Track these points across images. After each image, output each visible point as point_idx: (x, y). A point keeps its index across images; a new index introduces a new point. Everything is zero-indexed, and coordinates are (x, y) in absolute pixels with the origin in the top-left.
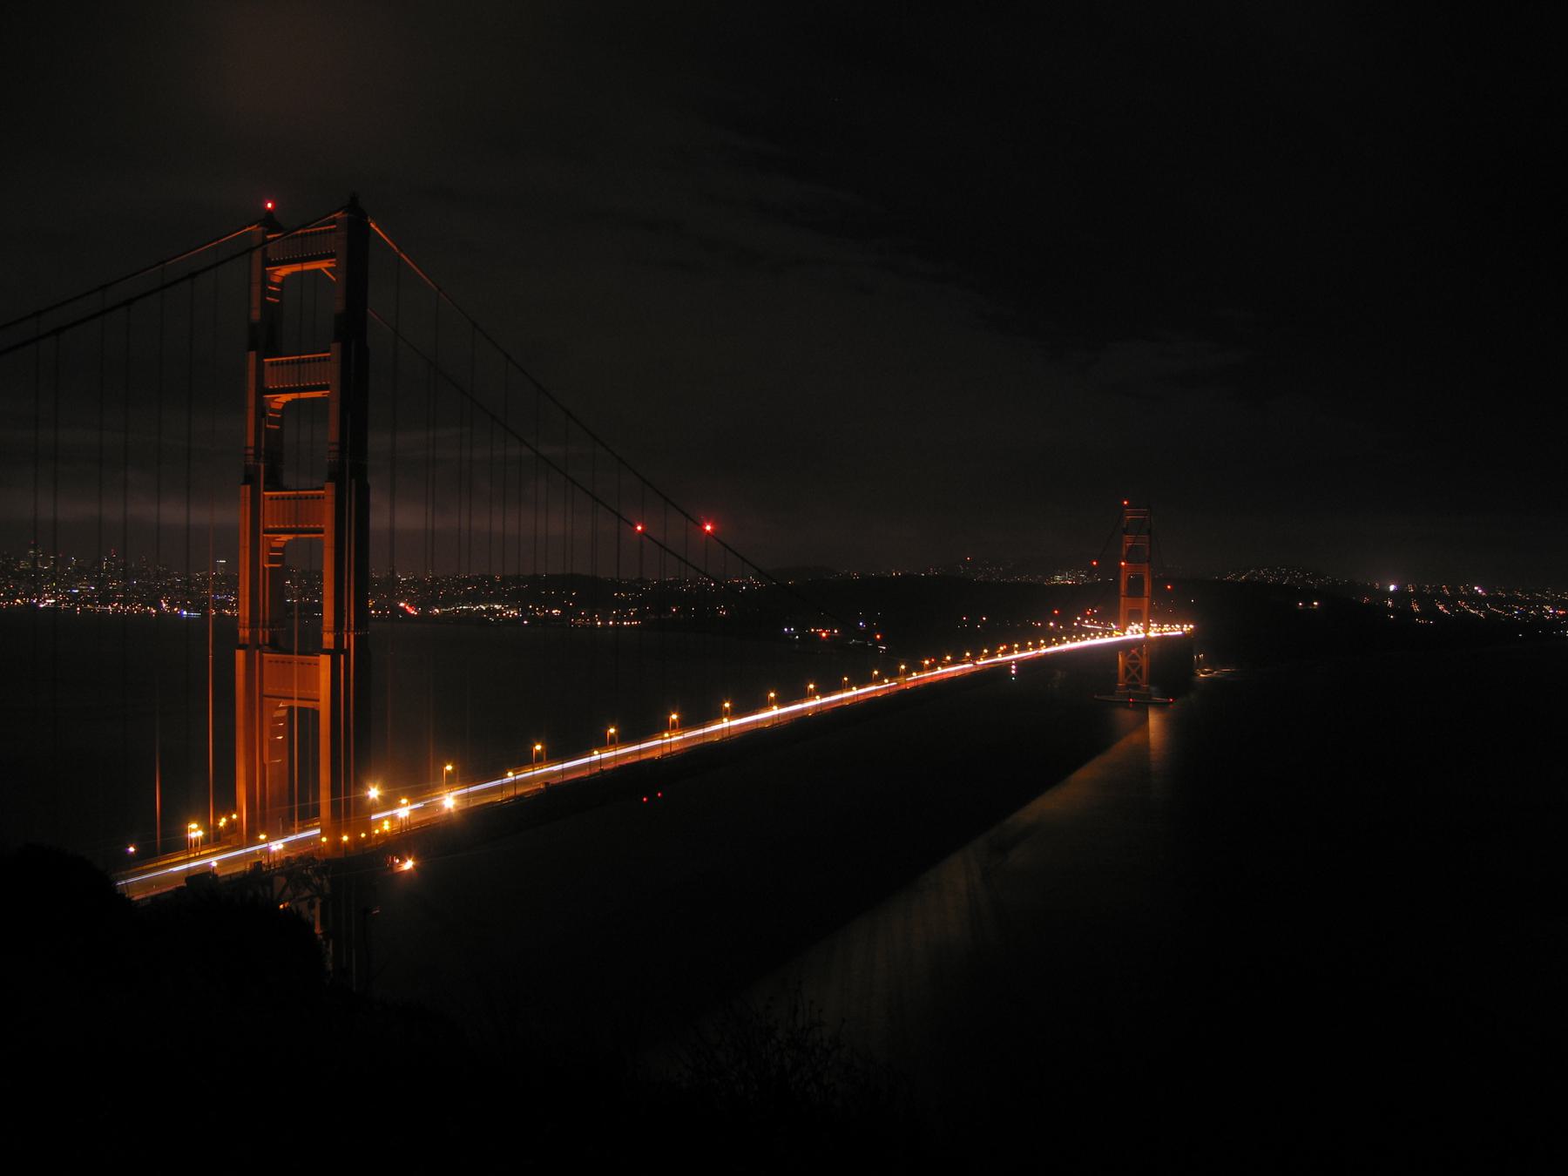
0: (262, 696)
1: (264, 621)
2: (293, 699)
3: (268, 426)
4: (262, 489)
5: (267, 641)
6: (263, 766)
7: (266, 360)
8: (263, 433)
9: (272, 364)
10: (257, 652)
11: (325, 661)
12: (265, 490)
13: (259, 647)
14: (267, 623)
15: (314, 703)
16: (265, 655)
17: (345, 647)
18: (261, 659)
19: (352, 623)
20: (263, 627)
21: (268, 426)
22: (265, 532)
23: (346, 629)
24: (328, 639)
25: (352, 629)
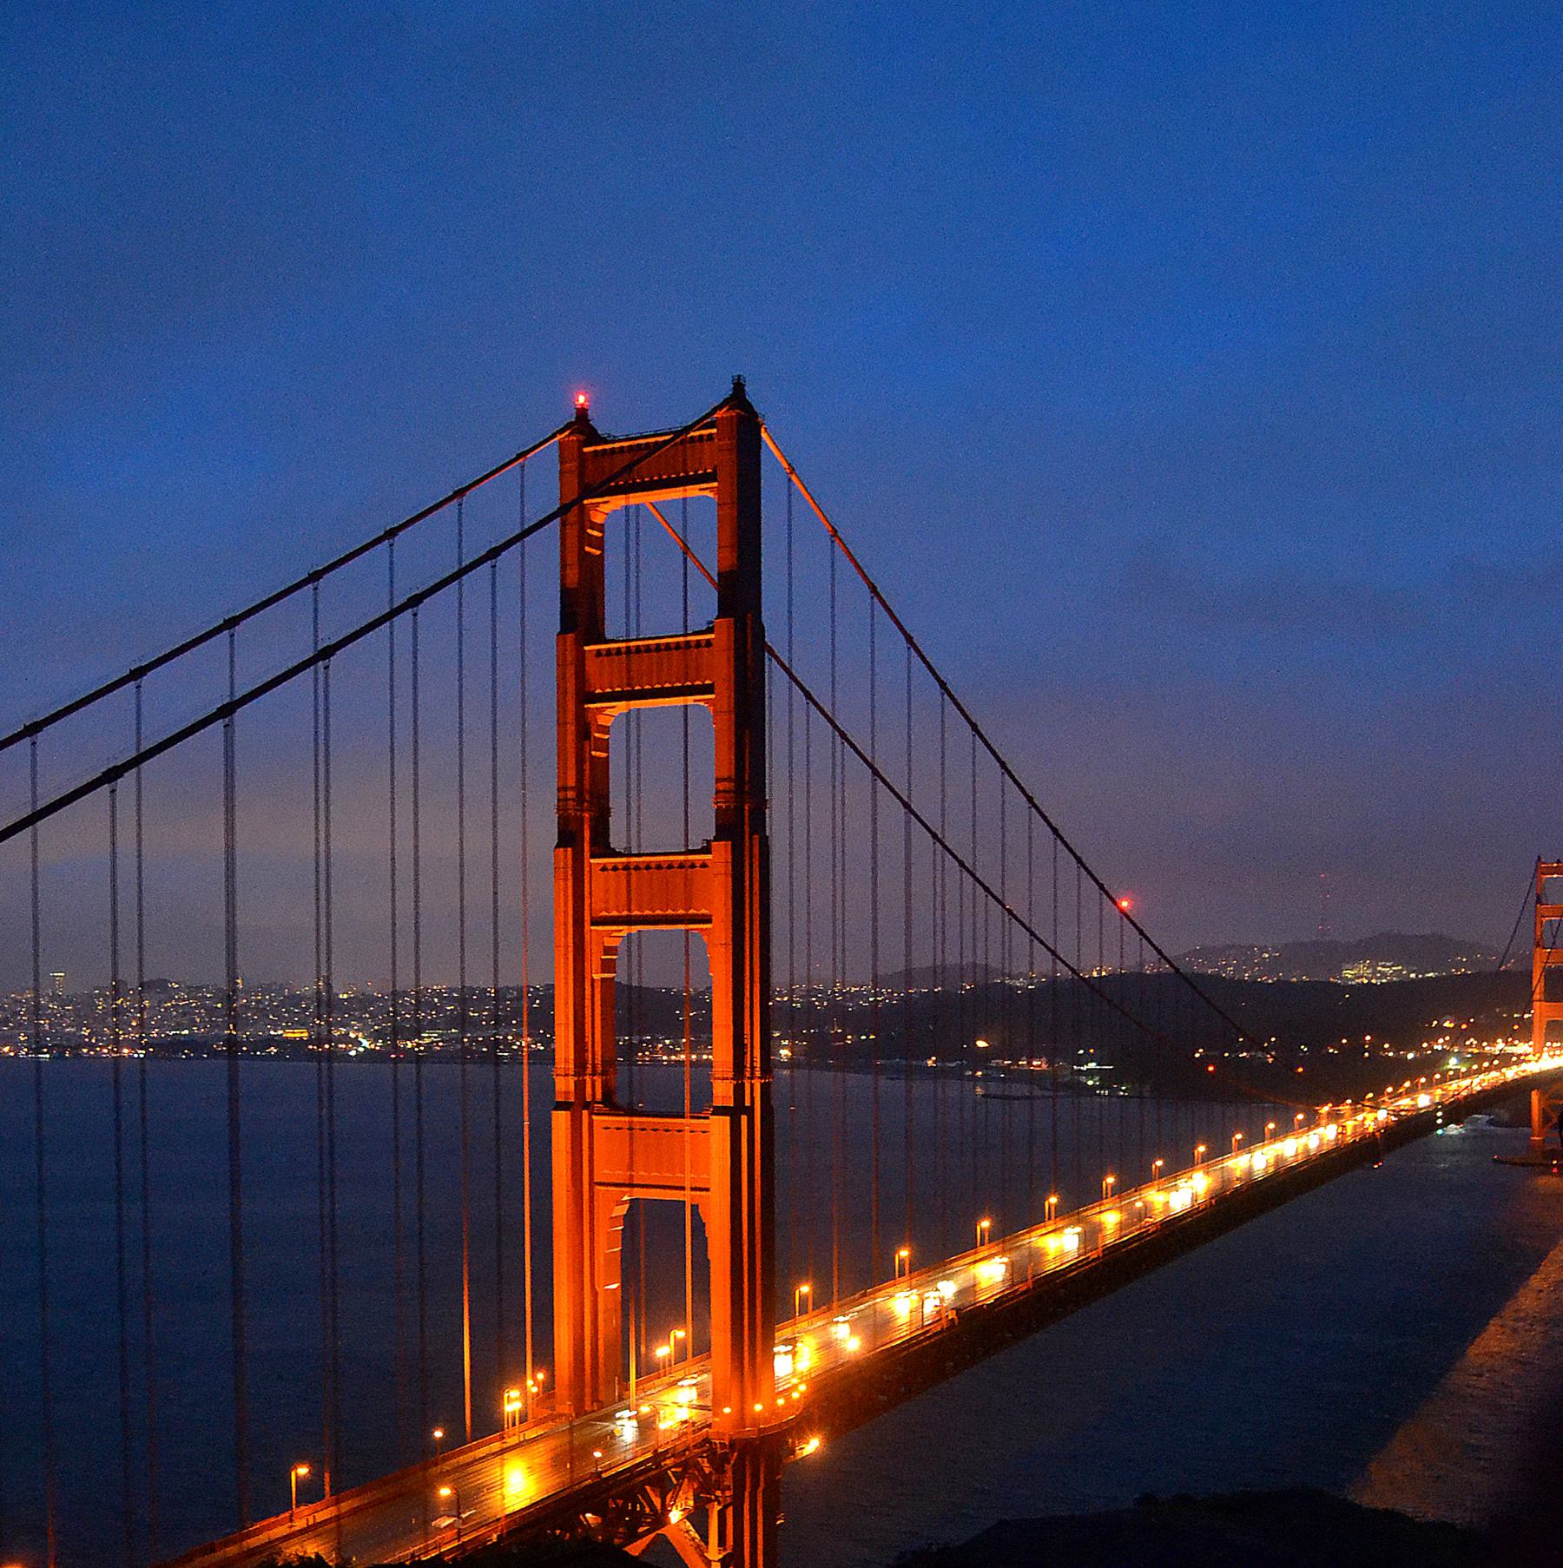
0: (592, 1184)
1: (594, 1065)
2: (683, 1188)
3: (593, 753)
4: (587, 854)
5: (599, 1096)
6: (595, 1294)
7: (586, 648)
8: (587, 767)
9: (599, 653)
10: (585, 1113)
11: (719, 1126)
12: (592, 856)
13: (587, 1106)
14: (599, 1069)
15: (704, 1193)
16: (594, 1117)
17: (747, 1104)
18: (591, 1123)
19: (758, 1064)
20: (593, 1074)
21: (593, 753)
22: (592, 924)
23: (748, 1075)
24: (723, 1092)
25: (758, 1074)
